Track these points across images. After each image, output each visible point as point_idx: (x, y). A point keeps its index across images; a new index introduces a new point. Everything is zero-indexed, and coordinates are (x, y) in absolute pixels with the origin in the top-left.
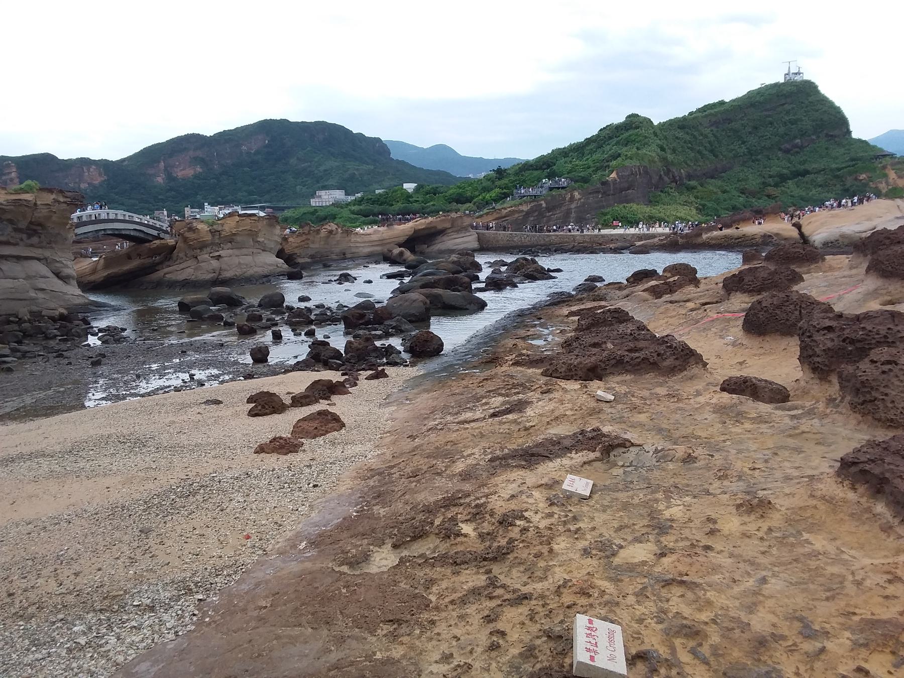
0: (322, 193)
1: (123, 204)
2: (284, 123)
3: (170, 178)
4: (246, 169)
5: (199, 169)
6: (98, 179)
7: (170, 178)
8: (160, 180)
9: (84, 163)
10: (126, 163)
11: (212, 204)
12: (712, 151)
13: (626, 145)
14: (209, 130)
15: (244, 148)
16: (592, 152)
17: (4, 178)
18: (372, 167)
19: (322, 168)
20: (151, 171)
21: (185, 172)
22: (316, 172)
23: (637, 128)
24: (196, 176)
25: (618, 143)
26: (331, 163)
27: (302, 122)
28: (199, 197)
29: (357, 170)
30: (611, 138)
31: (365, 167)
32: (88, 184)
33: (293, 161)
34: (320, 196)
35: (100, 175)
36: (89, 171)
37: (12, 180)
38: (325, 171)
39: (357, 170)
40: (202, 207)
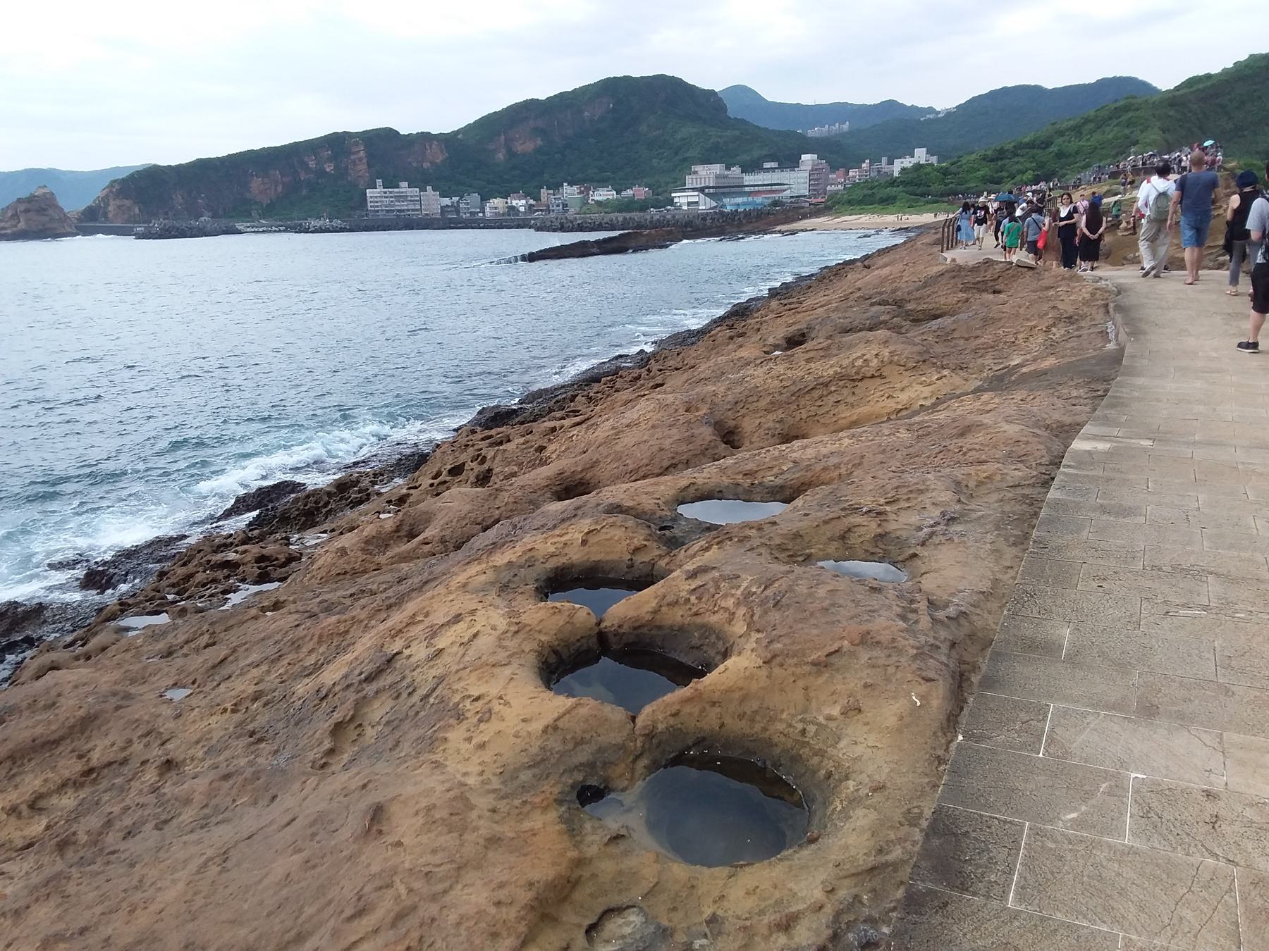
0: (699, 168)
1: (470, 186)
2: (627, 79)
3: (511, 153)
4: (592, 140)
5: (539, 142)
6: (438, 156)
7: (511, 153)
8: (500, 156)
9: (425, 137)
10: (460, 136)
11: (571, 184)
12: (1200, 128)
13: (1128, 126)
14: (542, 96)
15: (586, 114)
16: (1092, 132)
17: (352, 157)
18: (737, 133)
19: (679, 136)
20: (491, 147)
21: (525, 146)
22: (671, 141)
23: (1137, 110)
24: (538, 151)
25: (1117, 125)
26: (687, 130)
27: (642, 78)
28: (546, 176)
29: (721, 137)
30: (1110, 118)
31: (729, 133)
32: (431, 163)
33: (643, 128)
34: (696, 173)
35: (442, 151)
36: (431, 146)
37: (360, 159)
38: (683, 139)
39: (721, 137)
40: (556, 187)
